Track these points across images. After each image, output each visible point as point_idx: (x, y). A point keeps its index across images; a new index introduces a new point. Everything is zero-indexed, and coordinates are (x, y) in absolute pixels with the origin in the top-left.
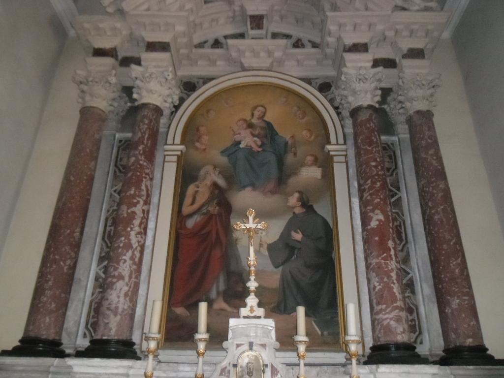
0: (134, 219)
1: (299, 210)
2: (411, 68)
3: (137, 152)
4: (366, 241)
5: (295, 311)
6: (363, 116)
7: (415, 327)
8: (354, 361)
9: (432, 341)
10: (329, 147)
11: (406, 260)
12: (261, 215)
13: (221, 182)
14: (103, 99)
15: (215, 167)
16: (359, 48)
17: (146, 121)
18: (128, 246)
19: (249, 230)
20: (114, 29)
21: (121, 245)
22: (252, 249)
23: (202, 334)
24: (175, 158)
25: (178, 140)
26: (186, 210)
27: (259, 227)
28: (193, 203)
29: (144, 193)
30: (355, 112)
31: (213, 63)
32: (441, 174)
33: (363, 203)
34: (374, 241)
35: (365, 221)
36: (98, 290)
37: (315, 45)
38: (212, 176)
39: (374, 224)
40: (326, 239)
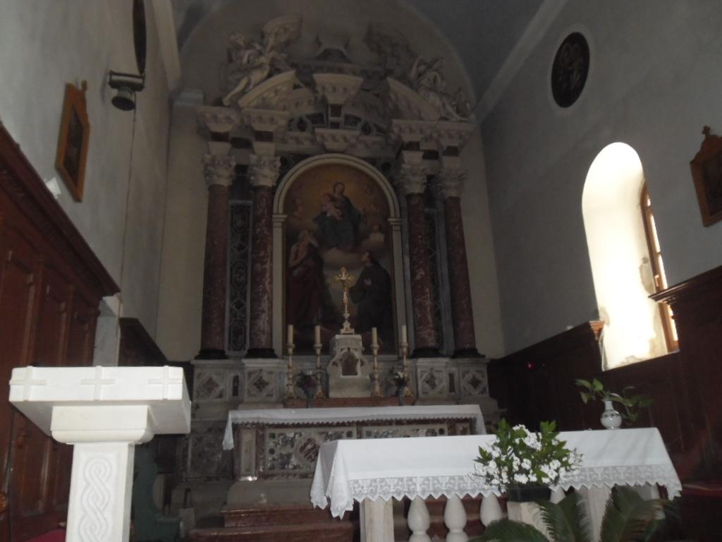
0: (265, 272)
1: (369, 265)
2: (448, 162)
3: (261, 224)
4: (413, 288)
5: (371, 331)
6: (415, 201)
7: (440, 339)
8: (405, 357)
9: (449, 345)
10: (390, 220)
11: (436, 298)
12: (350, 268)
13: (315, 243)
14: (224, 179)
15: (310, 231)
16: (413, 146)
17: (264, 200)
18: (265, 291)
19: (343, 281)
20: (228, 118)
21: (261, 290)
22: (345, 294)
23: (318, 344)
24: (280, 224)
25: (281, 211)
26: (292, 263)
27: (349, 278)
28: (296, 258)
29: (269, 254)
30: (409, 197)
31: (298, 141)
32: (462, 244)
33: (412, 263)
34: (417, 289)
35: (413, 275)
36: (233, 319)
37: (380, 130)
38: (307, 239)
39: (418, 277)
40: (386, 282)
